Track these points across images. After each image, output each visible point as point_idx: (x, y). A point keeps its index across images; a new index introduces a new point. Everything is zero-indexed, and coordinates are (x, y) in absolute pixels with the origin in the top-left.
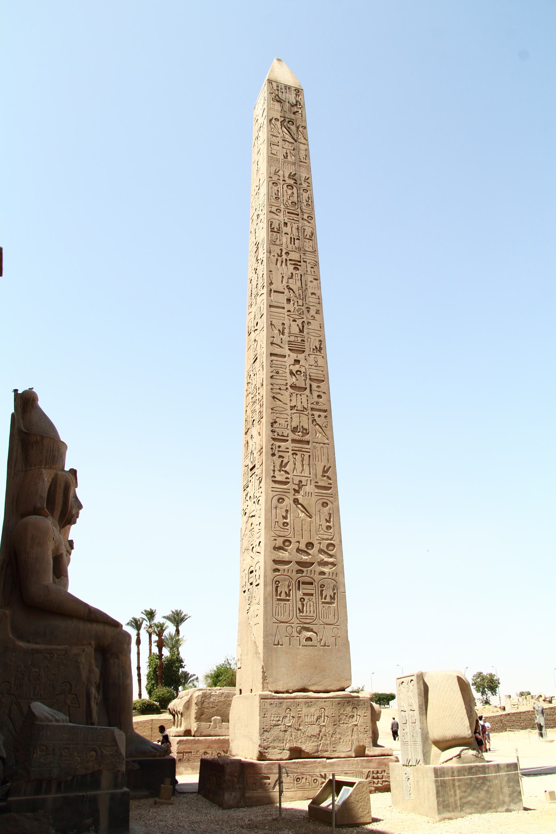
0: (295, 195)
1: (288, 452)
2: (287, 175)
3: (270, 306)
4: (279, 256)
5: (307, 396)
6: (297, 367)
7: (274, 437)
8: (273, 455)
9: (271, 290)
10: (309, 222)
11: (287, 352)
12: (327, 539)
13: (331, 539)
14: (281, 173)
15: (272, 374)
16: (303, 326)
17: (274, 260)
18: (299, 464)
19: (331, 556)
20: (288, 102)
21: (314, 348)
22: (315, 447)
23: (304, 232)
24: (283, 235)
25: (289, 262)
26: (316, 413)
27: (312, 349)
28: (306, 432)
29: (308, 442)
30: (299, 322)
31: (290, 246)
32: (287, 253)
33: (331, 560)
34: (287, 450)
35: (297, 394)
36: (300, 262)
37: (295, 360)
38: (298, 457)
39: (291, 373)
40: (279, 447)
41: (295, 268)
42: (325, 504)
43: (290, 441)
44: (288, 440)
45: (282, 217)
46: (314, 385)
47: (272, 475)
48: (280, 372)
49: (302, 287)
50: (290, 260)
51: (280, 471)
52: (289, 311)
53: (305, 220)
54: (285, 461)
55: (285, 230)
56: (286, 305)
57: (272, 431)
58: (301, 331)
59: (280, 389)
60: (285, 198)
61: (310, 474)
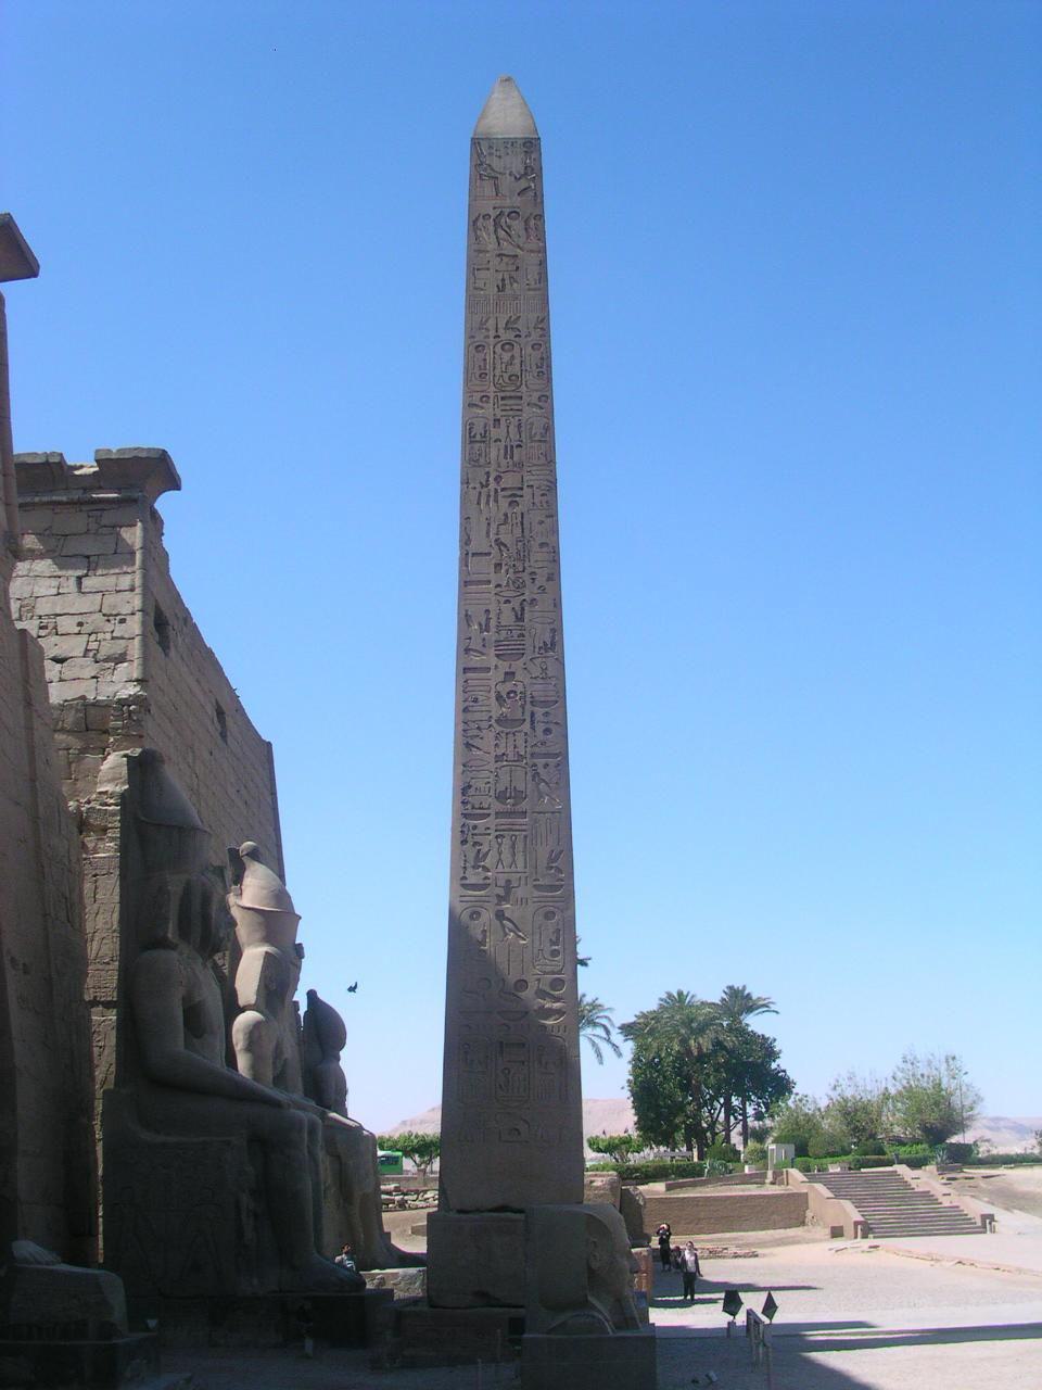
0: (517, 361)
1: (489, 834)
2: (501, 325)
3: (466, 582)
4: (482, 486)
5: (526, 734)
6: (509, 686)
7: (466, 812)
8: (464, 842)
9: (467, 554)
10: (541, 408)
11: (494, 661)
12: (553, 973)
13: (559, 972)
14: (491, 323)
15: (467, 704)
16: (523, 609)
17: (473, 495)
18: (506, 857)
19: (557, 999)
20: (510, 175)
21: (541, 645)
22: (536, 821)
23: (531, 428)
24: (493, 444)
25: (501, 494)
26: (540, 762)
27: (537, 650)
28: (519, 796)
29: (524, 814)
30: (516, 603)
31: (504, 462)
32: (498, 479)
33: (557, 1005)
34: (488, 831)
35: (507, 734)
36: (522, 489)
37: (506, 673)
38: (506, 842)
39: (499, 697)
40: (475, 827)
41: (510, 504)
42: (549, 915)
43: (492, 817)
44: (489, 815)
45: (491, 410)
46: (539, 711)
47: (462, 875)
48: (480, 698)
49: (523, 536)
50: (503, 490)
51: (473, 867)
52: (499, 586)
53: (536, 405)
54: (485, 849)
55: (494, 433)
56: (492, 576)
57: (463, 802)
58: (520, 618)
59: (478, 728)
60: (498, 372)
61: (526, 867)
